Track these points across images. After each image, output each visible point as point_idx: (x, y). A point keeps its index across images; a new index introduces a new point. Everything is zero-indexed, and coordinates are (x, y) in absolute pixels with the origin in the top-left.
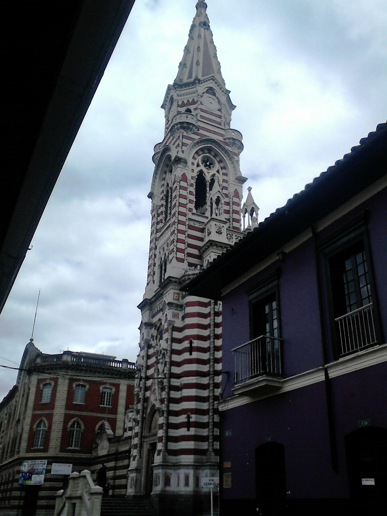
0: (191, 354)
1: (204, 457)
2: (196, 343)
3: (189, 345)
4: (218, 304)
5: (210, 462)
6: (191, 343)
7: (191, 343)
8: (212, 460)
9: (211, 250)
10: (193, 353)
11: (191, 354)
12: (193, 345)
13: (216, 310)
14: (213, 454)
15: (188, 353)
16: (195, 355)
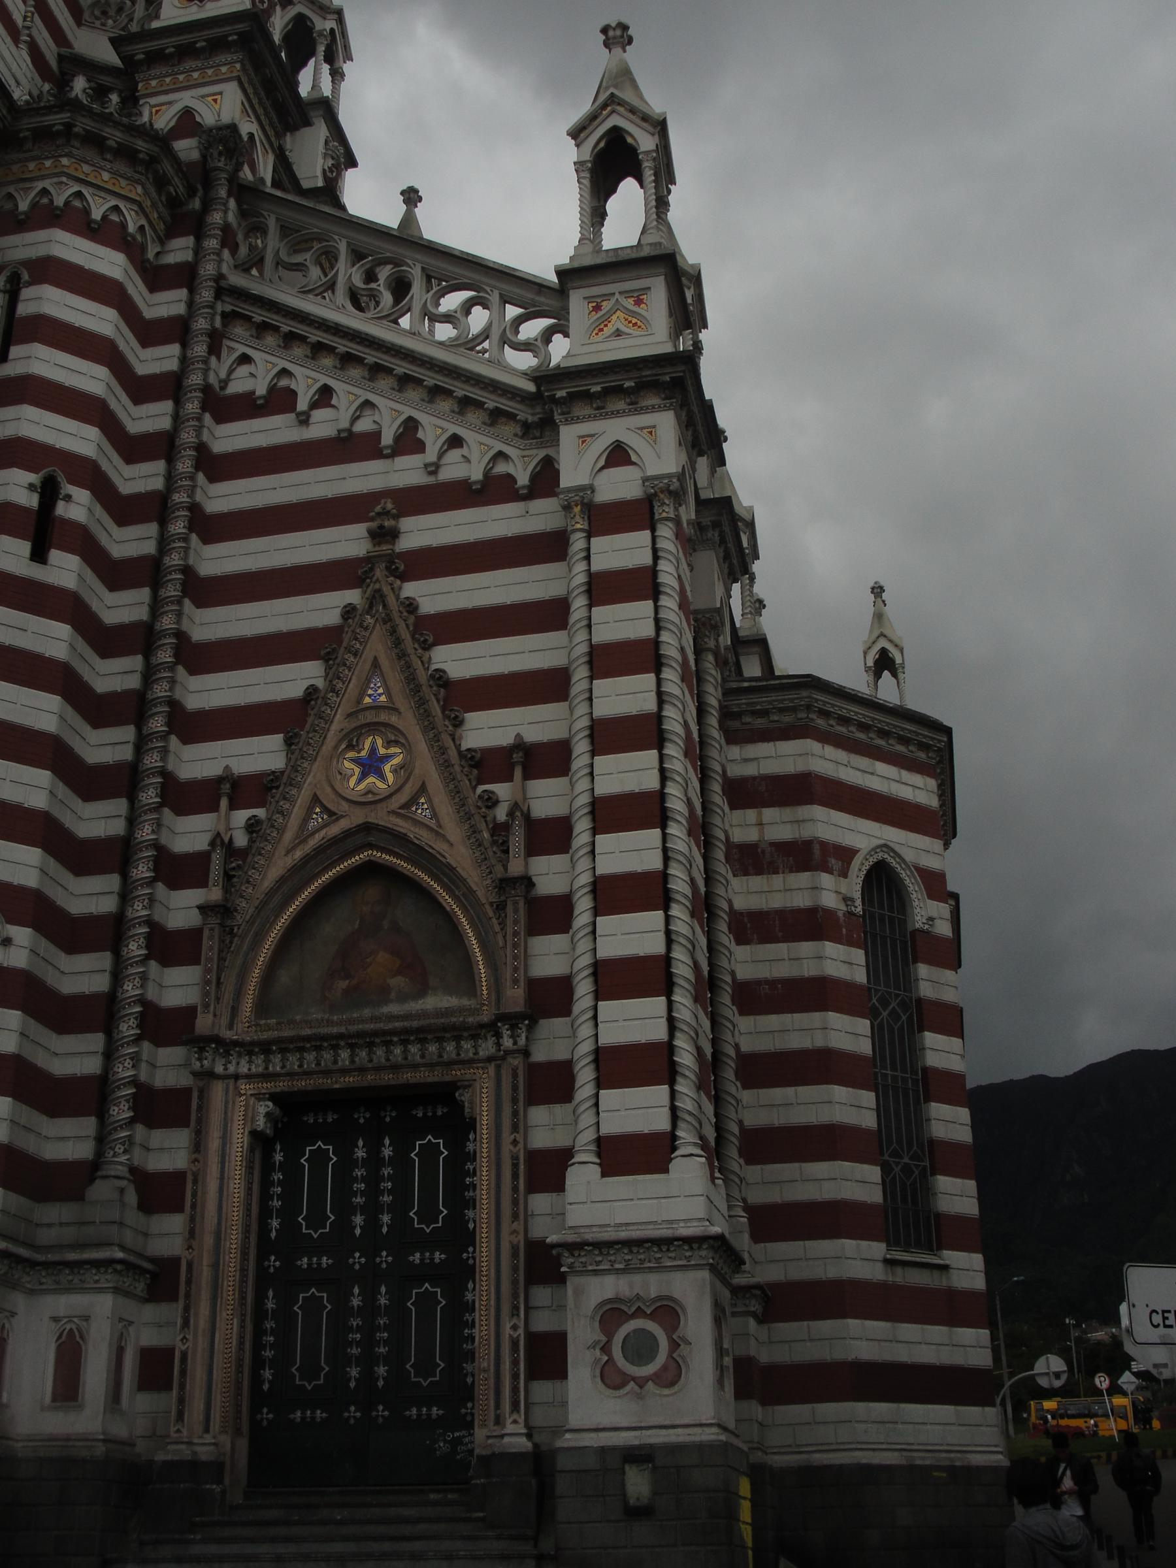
0: (39, 555)
1: (54, 1212)
2: (77, 505)
3: (32, 501)
4: (228, 360)
5: (123, 1248)
6: (49, 492)
7: (49, 492)
8: (129, 1237)
9: (230, 63)
10: (55, 555)
11: (39, 555)
12: (61, 509)
13: (212, 379)
14: (132, 1198)
15: (24, 547)
16: (65, 570)
